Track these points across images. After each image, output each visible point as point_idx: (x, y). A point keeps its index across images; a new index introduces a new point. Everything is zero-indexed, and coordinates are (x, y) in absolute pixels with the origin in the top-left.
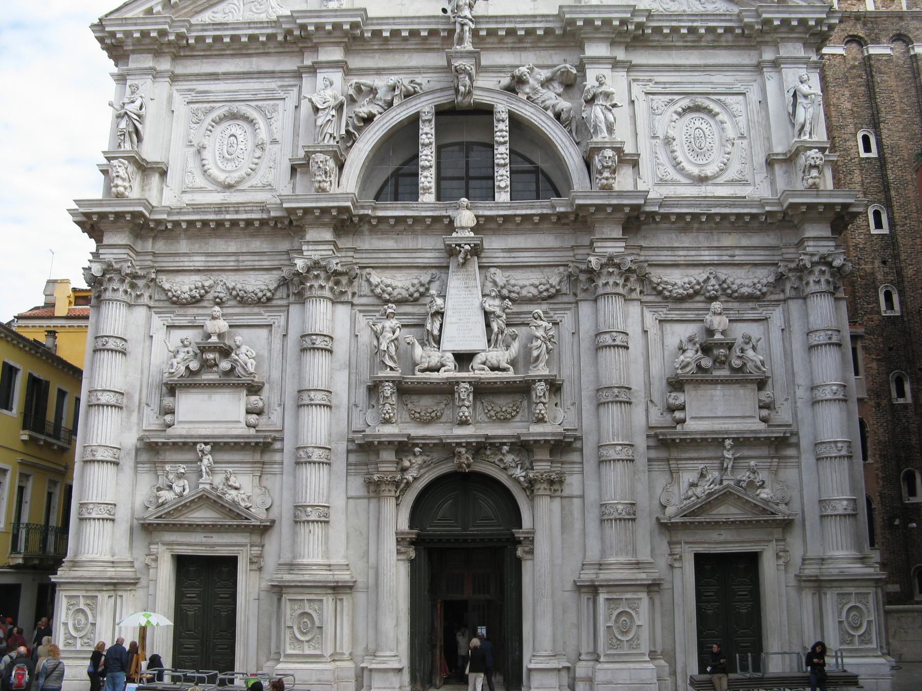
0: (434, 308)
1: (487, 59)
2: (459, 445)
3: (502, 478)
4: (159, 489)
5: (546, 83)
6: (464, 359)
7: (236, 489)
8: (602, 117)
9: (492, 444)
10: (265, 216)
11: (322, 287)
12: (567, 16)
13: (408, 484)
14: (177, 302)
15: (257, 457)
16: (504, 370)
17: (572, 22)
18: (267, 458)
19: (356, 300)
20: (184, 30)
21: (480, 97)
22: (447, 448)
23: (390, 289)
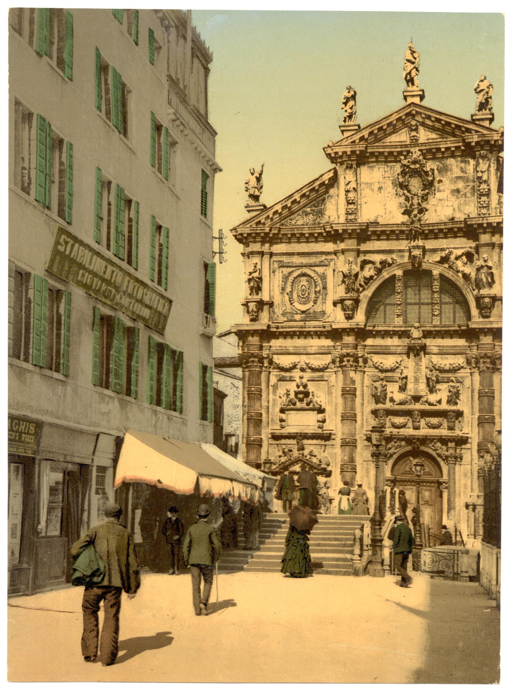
0: (404, 375)
1: (430, 244)
2: (414, 439)
3: (434, 453)
4: (280, 456)
5: (457, 258)
6: (417, 399)
7: (315, 456)
8: (484, 280)
9: (429, 439)
10: (322, 329)
11: (352, 366)
12: (468, 223)
13: (391, 456)
14: (282, 369)
15: (323, 442)
16: (435, 405)
17: (472, 225)
18: (327, 443)
19: (366, 369)
20: (276, 232)
21: (425, 266)
22: (409, 440)
23: (381, 365)
